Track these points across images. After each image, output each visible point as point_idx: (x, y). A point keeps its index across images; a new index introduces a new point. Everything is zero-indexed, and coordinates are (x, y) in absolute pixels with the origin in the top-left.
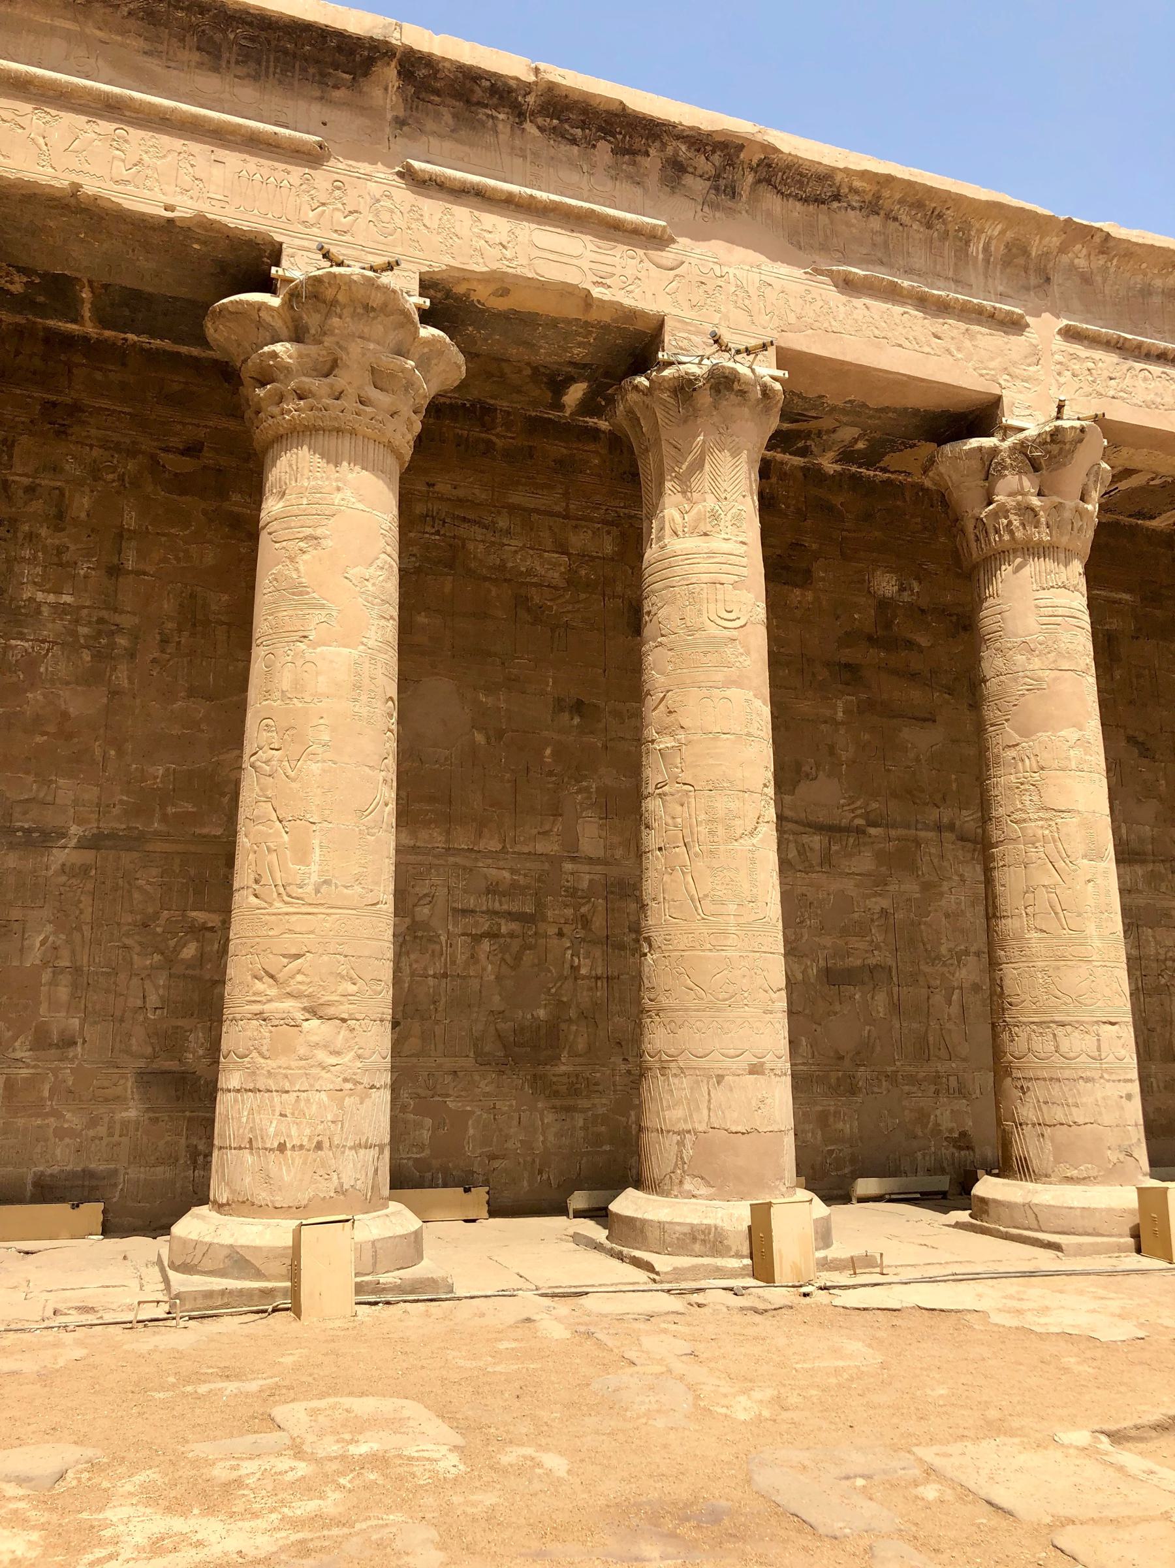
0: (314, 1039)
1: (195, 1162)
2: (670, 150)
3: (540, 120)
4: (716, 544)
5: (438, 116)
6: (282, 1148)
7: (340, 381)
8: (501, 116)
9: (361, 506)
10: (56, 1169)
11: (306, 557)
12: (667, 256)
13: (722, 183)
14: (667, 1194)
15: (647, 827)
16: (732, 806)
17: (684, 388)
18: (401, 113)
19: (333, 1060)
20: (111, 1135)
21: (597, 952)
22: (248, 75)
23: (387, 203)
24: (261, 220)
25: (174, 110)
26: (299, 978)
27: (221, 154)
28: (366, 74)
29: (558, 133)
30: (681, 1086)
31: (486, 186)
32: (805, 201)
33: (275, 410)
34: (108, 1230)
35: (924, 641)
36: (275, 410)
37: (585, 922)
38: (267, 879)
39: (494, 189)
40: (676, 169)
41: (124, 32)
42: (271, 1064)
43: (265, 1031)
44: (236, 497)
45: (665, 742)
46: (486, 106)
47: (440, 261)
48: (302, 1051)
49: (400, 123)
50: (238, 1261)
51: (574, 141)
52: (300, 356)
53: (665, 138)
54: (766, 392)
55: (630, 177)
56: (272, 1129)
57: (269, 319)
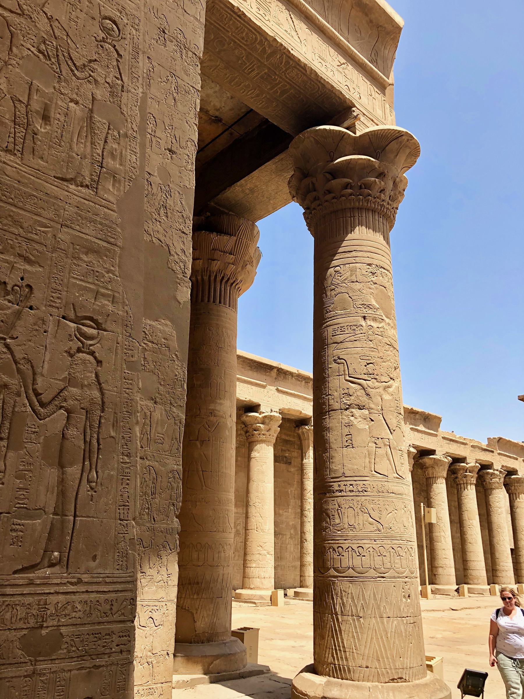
5: (281, 377)
6: (264, 578)
27: (253, 387)
49: (276, 379)
50: (261, 597)
56: (262, 574)
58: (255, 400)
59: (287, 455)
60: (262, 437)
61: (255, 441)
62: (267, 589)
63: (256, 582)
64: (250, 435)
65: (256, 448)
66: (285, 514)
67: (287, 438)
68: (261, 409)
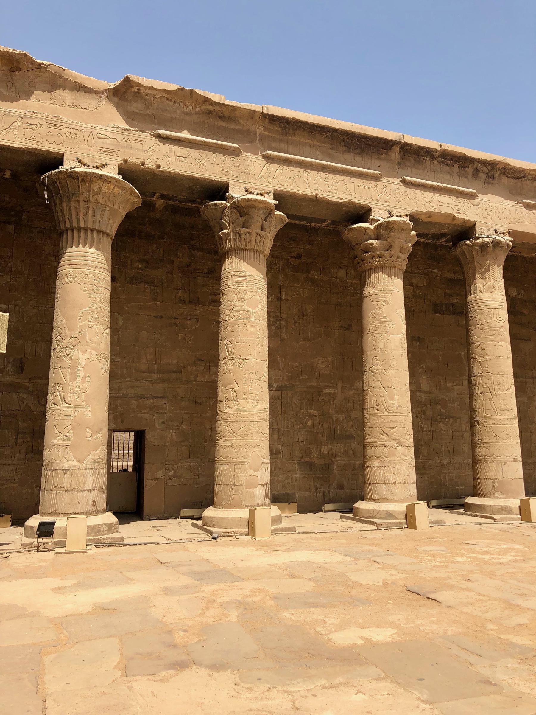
0: (401, 452)
1: (316, 491)
2: (475, 166)
3: (438, 159)
4: (495, 296)
5: (410, 160)
6: (395, 483)
7: (392, 252)
8: (428, 159)
9: (398, 290)
10: (278, 493)
11: (384, 307)
12: (475, 201)
13: (490, 175)
14: (489, 497)
15: (475, 386)
16: (505, 380)
17: (484, 246)
18: (400, 161)
19: (405, 458)
20: (292, 482)
21: (429, 422)
22: (358, 153)
23: (398, 191)
24: (365, 200)
25: (341, 168)
26: (395, 434)
27: (354, 180)
28: (390, 150)
29: (443, 163)
30: (493, 466)
31: (426, 183)
32: (514, 178)
33: (372, 261)
34: (299, 511)
35: (526, 312)
36: (372, 261)
37: (424, 412)
38: (381, 405)
39: (428, 184)
40: (477, 171)
41: (324, 143)
42: (389, 459)
43: (386, 450)
44: (312, 273)
45: (481, 359)
46: (423, 156)
47: (413, 209)
48: (398, 456)
49: (400, 164)
50: (389, 515)
51: (447, 165)
52: (380, 244)
53: (475, 162)
54: (508, 245)
55: (463, 175)
56: (391, 478)
57: (369, 232)
58: (360, 199)
59: (455, 301)
60: (378, 261)
61: (368, 270)
62: (401, 501)
63: (383, 490)
64: (360, 261)
65: (369, 281)
66: (456, 388)
67: (453, 277)
68: (373, 214)
